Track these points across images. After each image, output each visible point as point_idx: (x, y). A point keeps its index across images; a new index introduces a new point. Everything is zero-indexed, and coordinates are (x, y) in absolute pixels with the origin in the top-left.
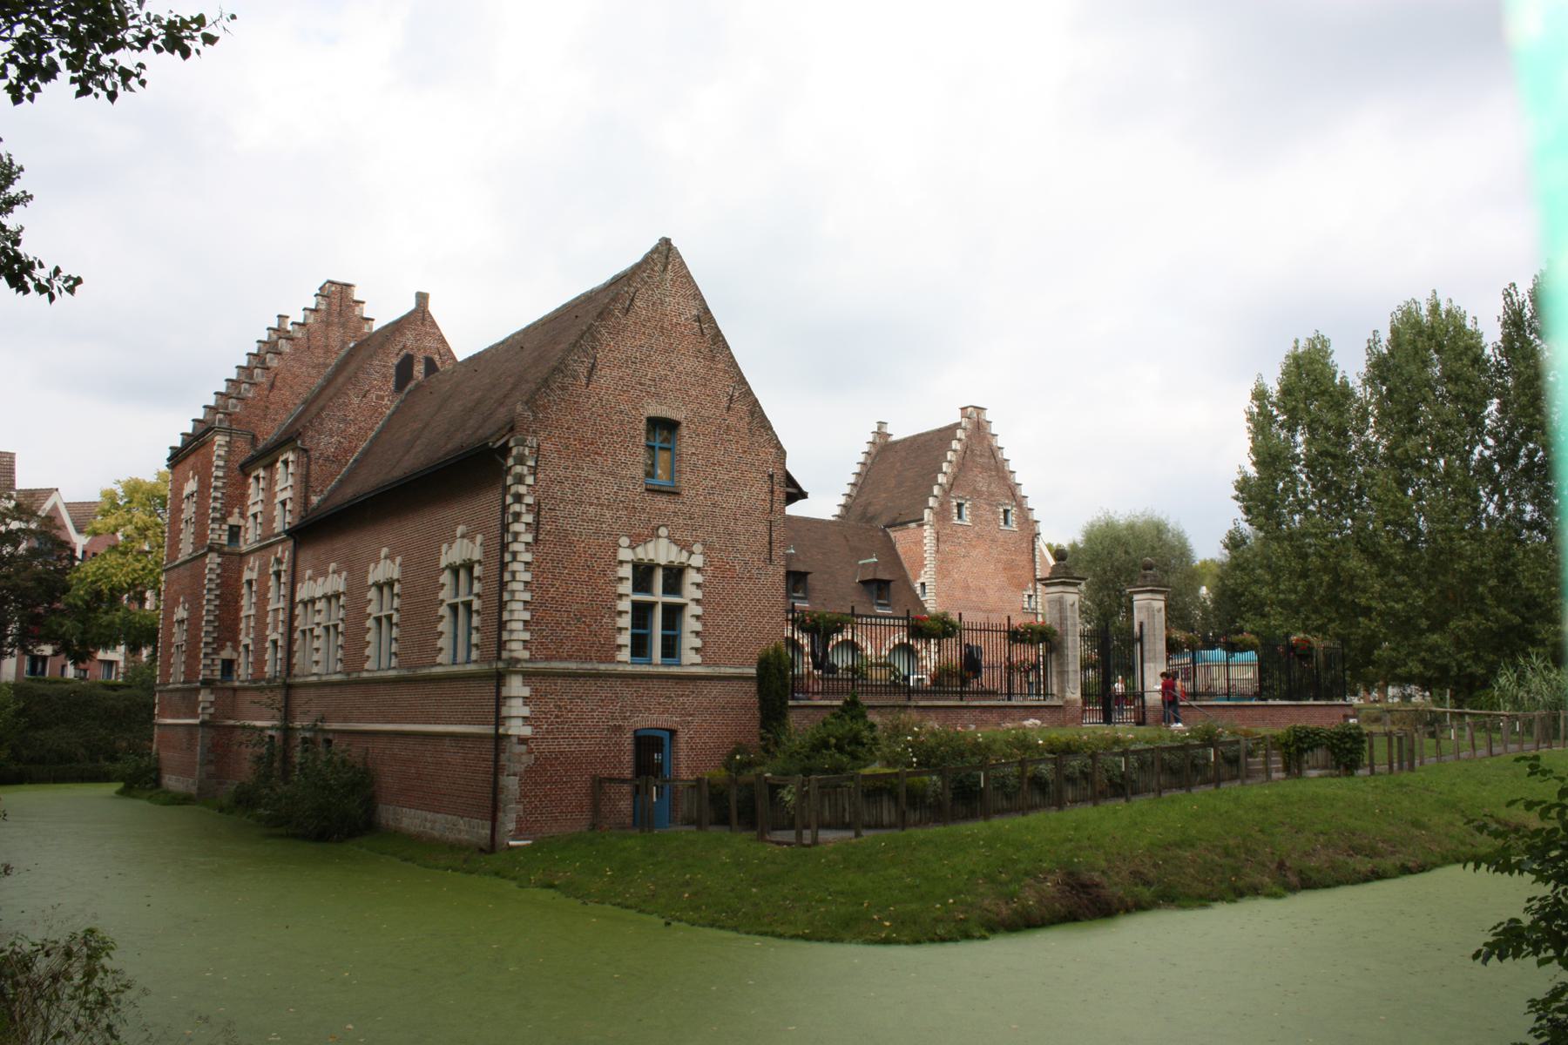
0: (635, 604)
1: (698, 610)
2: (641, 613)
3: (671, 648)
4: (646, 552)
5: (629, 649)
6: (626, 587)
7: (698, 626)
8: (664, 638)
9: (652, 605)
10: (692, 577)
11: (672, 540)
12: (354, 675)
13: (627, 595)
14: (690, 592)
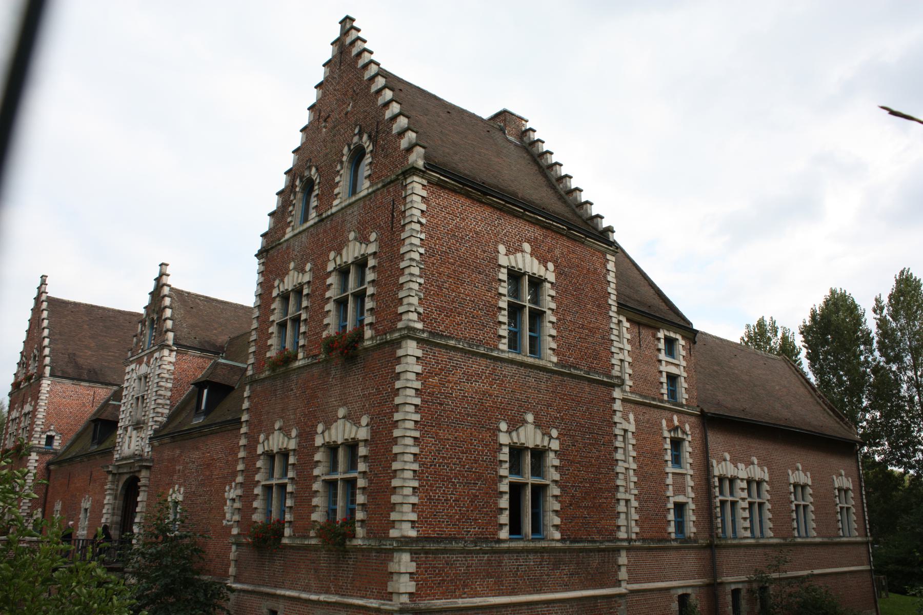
0: (512, 485)
2: (516, 490)
5: (507, 528)
6: (504, 471)
7: (557, 506)
10: (552, 460)
11: (537, 424)
12: (789, 540)
13: (506, 477)
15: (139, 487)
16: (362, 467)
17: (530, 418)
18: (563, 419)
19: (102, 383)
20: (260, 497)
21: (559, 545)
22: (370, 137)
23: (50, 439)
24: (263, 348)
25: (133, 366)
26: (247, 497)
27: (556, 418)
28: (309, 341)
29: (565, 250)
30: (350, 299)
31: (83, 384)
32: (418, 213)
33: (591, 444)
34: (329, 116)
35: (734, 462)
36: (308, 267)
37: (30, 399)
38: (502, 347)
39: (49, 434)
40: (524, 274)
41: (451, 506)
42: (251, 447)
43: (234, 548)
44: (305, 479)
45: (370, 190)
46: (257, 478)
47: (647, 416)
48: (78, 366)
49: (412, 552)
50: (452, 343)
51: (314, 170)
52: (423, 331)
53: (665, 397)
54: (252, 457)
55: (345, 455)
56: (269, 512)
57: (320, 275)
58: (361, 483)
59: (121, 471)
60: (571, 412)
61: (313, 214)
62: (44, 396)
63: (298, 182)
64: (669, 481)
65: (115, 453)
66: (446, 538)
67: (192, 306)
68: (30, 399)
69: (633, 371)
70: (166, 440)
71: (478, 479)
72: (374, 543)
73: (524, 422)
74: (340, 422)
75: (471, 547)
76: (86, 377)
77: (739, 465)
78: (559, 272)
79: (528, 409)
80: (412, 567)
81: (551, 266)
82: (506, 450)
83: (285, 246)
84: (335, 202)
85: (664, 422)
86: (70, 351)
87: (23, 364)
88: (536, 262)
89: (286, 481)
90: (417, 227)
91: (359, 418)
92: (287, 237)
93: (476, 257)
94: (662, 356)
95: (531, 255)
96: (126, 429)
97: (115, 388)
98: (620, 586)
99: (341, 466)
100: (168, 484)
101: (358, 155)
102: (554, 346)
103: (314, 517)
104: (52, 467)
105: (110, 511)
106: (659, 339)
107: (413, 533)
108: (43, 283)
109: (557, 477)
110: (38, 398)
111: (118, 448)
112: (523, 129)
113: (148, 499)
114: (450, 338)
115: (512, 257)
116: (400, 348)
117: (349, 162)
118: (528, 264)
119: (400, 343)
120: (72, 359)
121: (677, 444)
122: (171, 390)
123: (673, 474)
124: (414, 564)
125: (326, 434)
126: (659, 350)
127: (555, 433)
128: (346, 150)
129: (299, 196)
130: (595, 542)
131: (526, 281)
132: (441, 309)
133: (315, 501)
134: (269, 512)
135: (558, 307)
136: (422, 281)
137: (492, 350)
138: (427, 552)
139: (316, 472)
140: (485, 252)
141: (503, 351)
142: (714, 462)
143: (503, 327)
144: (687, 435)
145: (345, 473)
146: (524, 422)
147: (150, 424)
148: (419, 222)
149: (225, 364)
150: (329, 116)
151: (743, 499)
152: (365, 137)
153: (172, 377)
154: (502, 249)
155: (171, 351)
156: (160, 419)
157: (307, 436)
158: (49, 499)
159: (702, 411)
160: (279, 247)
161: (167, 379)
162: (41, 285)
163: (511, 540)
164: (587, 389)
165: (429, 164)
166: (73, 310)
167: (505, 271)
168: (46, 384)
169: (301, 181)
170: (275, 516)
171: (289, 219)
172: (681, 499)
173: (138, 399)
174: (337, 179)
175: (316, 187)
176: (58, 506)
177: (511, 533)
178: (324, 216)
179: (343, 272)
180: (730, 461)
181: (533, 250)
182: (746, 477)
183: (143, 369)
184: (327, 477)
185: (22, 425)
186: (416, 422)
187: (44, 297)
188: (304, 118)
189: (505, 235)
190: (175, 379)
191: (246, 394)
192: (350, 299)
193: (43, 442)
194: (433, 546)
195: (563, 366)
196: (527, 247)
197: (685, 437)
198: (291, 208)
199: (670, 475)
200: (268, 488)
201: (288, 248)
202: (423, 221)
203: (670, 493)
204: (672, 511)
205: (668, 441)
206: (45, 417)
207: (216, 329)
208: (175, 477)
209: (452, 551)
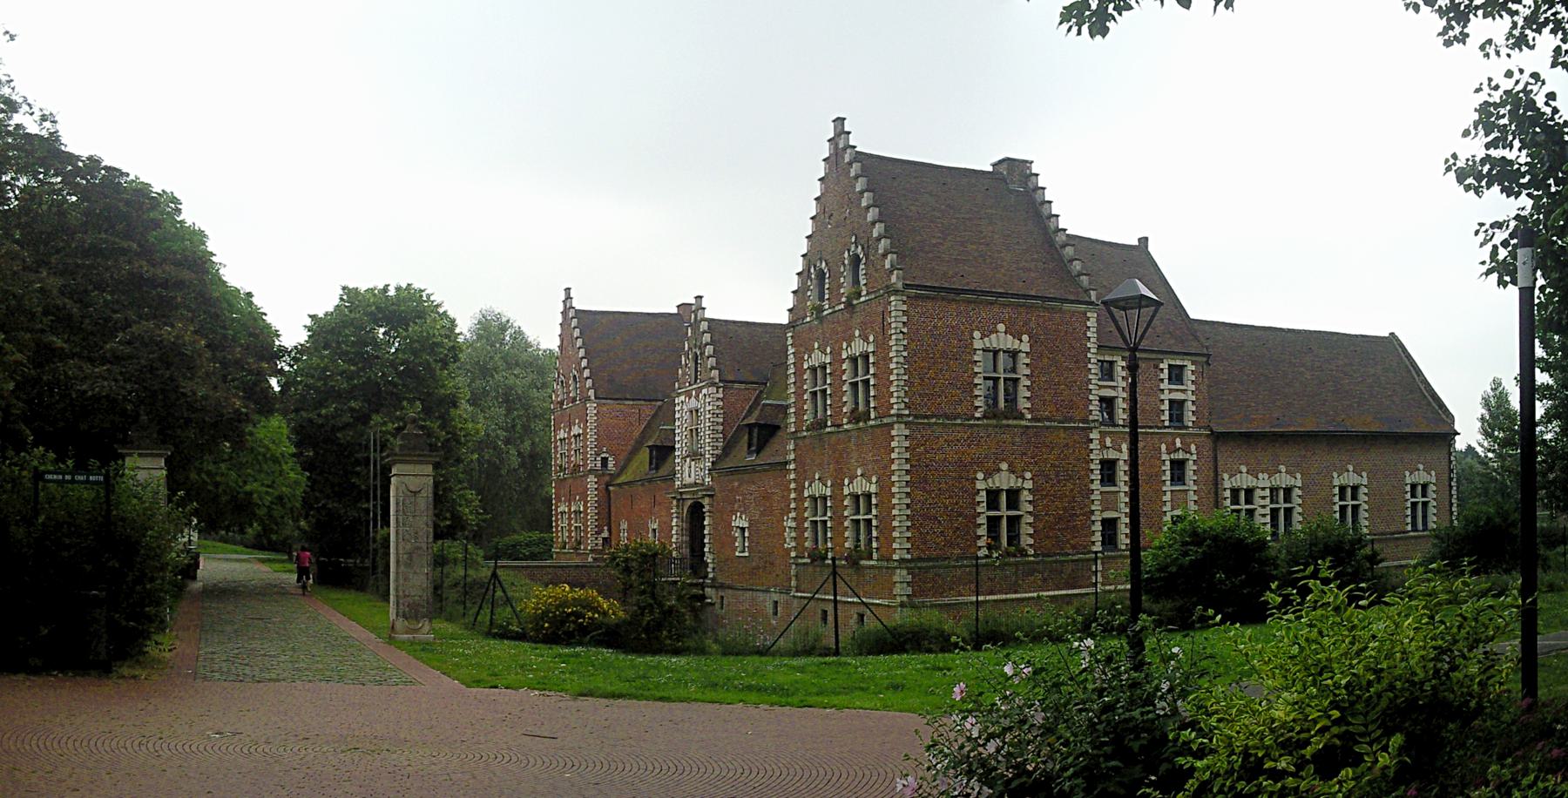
1: (1031, 520)
2: (993, 523)
4: (994, 483)
11: (1012, 470)
16: (874, 512)
17: (1004, 466)
21: (1032, 559)
22: (863, 248)
23: (605, 461)
24: (800, 413)
25: (682, 398)
26: (799, 529)
32: (901, 325)
35: (1253, 472)
36: (828, 350)
40: (1000, 350)
42: (799, 490)
43: (794, 567)
44: (839, 519)
49: (907, 568)
52: (909, 416)
53: (1167, 423)
54: (800, 499)
57: (837, 359)
58: (874, 523)
59: (684, 496)
62: (592, 418)
63: (812, 270)
71: (960, 516)
73: (999, 470)
74: (859, 478)
78: (1034, 341)
81: (1025, 338)
82: (984, 493)
85: (1163, 447)
90: (901, 336)
94: (1165, 385)
95: (1006, 333)
96: (684, 459)
97: (659, 403)
99: (862, 511)
101: (856, 260)
104: (611, 488)
107: (909, 557)
108: (568, 297)
115: (986, 339)
121: (1178, 466)
123: (1172, 491)
127: (1028, 475)
128: (846, 255)
135: (1032, 371)
136: (906, 377)
138: (919, 568)
139: (846, 514)
146: (999, 470)
147: (707, 456)
148: (901, 332)
151: (1264, 507)
152: (860, 247)
154: (977, 334)
156: (716, 452)
157: (838, 485)
159: (1211, 431)
162: (566, 299)
164: (1062, 435)
168: (591, 407)
173: (691, 430)
174: (842, 280)
176: (624, 526)
179: (854, 360)
182: (1269, 485)
183: (693, 403)
184: (855, 517)
185: (573, 446)
186: (907, 482)
189: (980, 322)
190: (724, 413)
194: (924, 565)
197: (1188, 456)
202: (905, 330)
203: (1167, 508)
205: (1168, 463)
208: (736, 506)
209: (940, 567)
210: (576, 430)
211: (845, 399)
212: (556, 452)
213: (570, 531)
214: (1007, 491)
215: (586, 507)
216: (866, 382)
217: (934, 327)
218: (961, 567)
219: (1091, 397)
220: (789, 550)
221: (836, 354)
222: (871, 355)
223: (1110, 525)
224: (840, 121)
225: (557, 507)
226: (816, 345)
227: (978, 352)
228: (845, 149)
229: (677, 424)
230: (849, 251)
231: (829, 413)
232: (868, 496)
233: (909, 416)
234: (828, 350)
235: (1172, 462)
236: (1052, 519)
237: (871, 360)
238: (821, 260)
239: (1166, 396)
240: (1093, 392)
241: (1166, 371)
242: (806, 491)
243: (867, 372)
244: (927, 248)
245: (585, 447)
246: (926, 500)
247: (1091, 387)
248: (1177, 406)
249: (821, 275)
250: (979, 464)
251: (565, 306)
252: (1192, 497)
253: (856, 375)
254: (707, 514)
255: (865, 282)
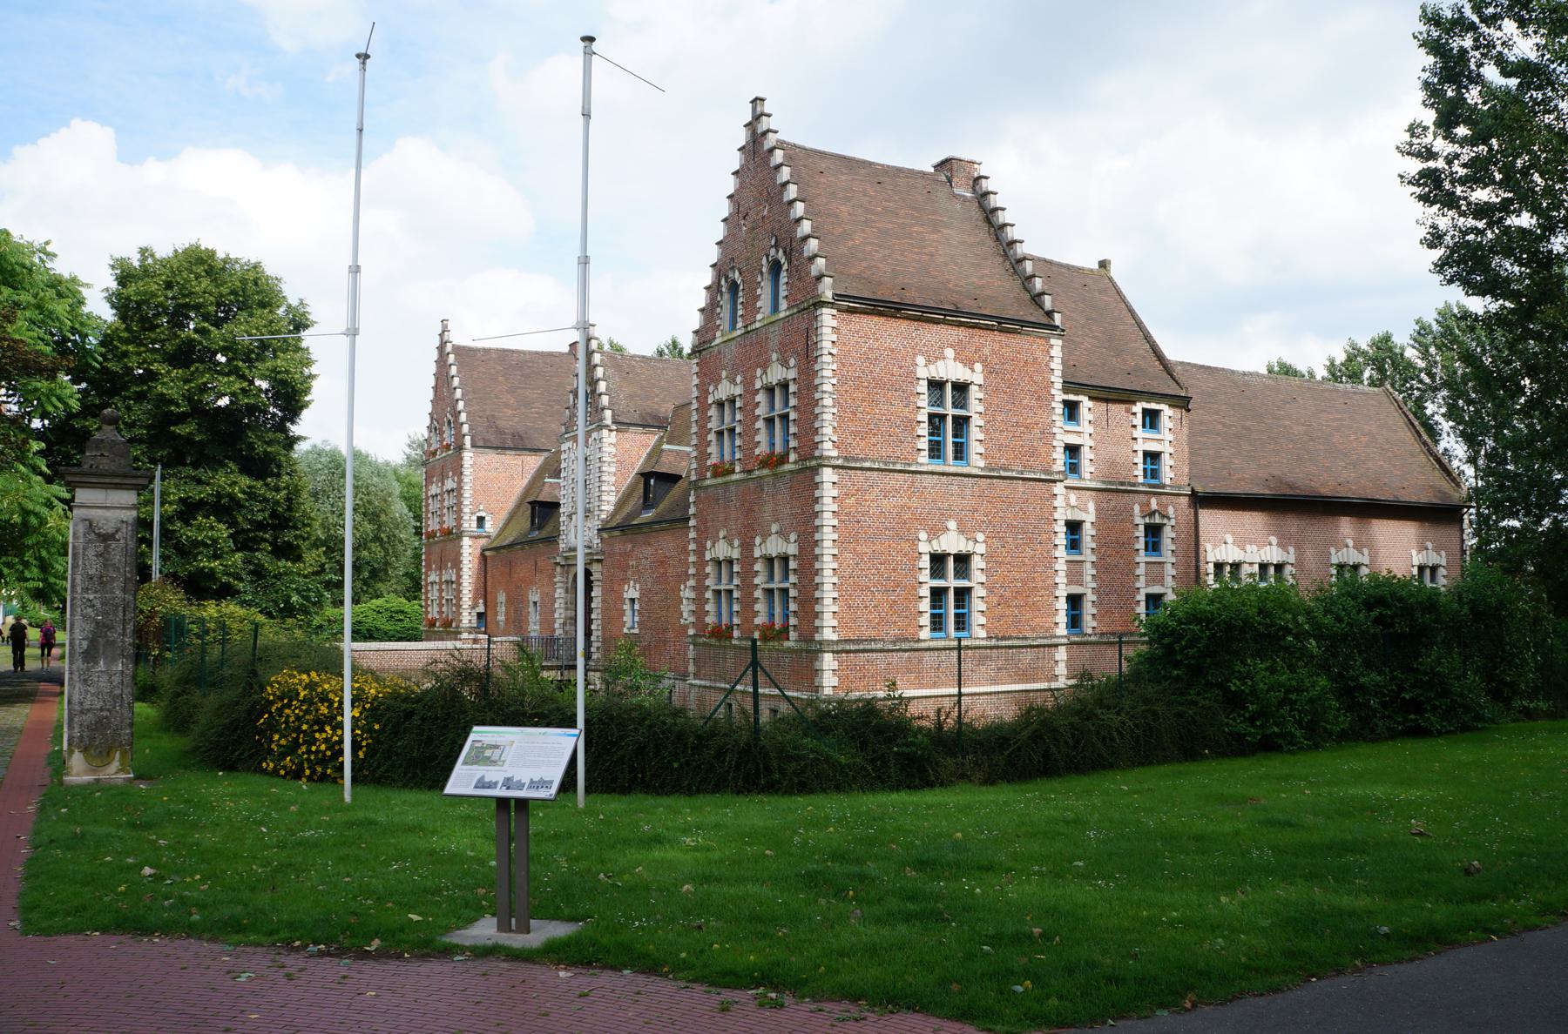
3: (962, 622)
6: (925, 576)
7: (983, 607)
8: (957, 615)
9: (945, 590)
10: (977, 563)
11: (961, 531)
14: (977, 577)
15: (592, 582)
16: (793, 579)
17: (952, 525)
18: (990, 522)
19: (530, 450)
20: (712, 601)
21: (984, 643)
22: (785, 252)
23: (481, 520)
26: (700, 601)
27: (983, 522)
28: (745, 455)
29: (997, 346)
30: (777, 420)
31: (508, 452)
33: (1024, 544)
34: (747, 214)
35: (1241, 543)
36: (739, 379)
37: (451, 474)
38: (920, 460)
39: (479, 514)
40: (947, 381)
41: (870, 612)
42: (700, 551)
43: (691, 647)
44: (748, 587)
45: (788, 313)
46: (707, 582)
47: (1113, 503)
48: (500, 432)
50: (867, 465)
51: (737, 273)
52: (838, 458)
53: (1141, 479)
54: (701, 564)
55: (780, 567)
56: (719, 614)
57: (750, 392)
58: (793, 593)
60: (1001, 514)
61: (740, 325)
62: (467, 471)
63: (723, 282)
64: (1141, 570)
65: (560, 542)
66: (866, 640)
67: (627, 370)
68: (451, 474)
69: (1096, 454)
70: (616, 533)
71: (897, 587)
72: (804, 646)
75: (891, 647)
76: (509, 443)
77: (1248, 547)
78: (989, 371)
79: (950, 516)
80: (835, 665)
81: (978, 367)
83: (716, 349)
84: (759, 317)
85: (1137, 508)
86: (488, 413)
87: (435, 429)
88: (960, 365)
89: (732, 587)
91: (788, 534)
92: (717, 341)
93: (893, 375)
94: (1139, 433)
97: (546, 454)
98: (1057, 680)
100: (622, 580)
101: (776, 267)
102: (982, 450)
103: (758, 621)
105: (562, 606)
106: (1134, 414)
109: (983, 579)
110: (461, 473)
111: (564, 537)
112: (976, 175)
113: (603, 594)
114: (863, 460)
115: (932, 367)
116: (817, 474)
117: (769, 273)
118: (951, 369)
119: (817, 470)
120: (491, 420)
121: (1154, 531)
122: (615, 474)
123: (1146, 563)
124: (836, 662)
125: (763, 546)
126: (1134, 426)
128: (764, 261)
129: (726, 296)
130: (1026, 638)
131: (949, 387)
132: (855, 434)
133: (758, 607)
134: (719, 614)
135: (986, 409)
136: (835, 411)
137: (909, 465)
139: (757, 581)
140: (901, 367)
141: (921, 464)
142: (1209, 547)
143: (922, 439)
144: (1169, 519)
145: (780, 582)
148: (830, 354)
149: (670, 451)
150: (747, 214)
152: (781, 251)
153: (614, 460)
154: (920, 360)
155: (611, 431)
157: (747, 547)
158: (489, 589)
160: (711, 350)
161: (609, 463)
162: (443, 332)
163: (932, 639)
164: (1021, 489)
165: (837, 295)
166: (483, 358)
167: (926, 382)
168: (468, 456)
169: (726, 281)
170: (725, 620)
171: (718, 322)
172: (1156, 590)
174: (759, 291)
175: (741, 294)
176: (502, 598)
177: (934, 630)
178: (749, 329)
179: (770, 390)
180: (1234, 543)
181: (957, 354)
184: (766, 586)
185: (446, 504)
187: (449, 348)
188: (725, 209)
191: (692, 499)
192: (777, 420)
193: (474, 524)
195: (990, 470)
196: (950, 353)
197: (1165, 521)
198: (718, 310)
199: (1142, 566)
200: (718, 593)
201: (719, 353)
202: (834, 351)
203: (1141, 583)
204: (1143, 604)
205: (1142, 528)
206: (472, 495)
207: (657, 396)
209: (872, 651)
210: (450, 484)
211: (757, 438)
212: (428, 511)
213: (441, 605)
214: (955, 555)
215: (459, 577)
216: (785, 417)
217: (870, 349)
218: (897, 651)
219: (1055, 443)
220: (686, 627)
221: (748, 383)
222: (791, 383)
223: (1074, 601)
224: (757, 101)
225: (427, 576)
226: (724, 374)
227: (921, 382)
228: (765, 133)
229: (562, 475)
230: (767, 256)
231: (737, 456)
232: (785, 559)
233: (838, 458)
234: (739, 379)
235: (1147, 527)
236: (1008, 594)
237: (792, 388)
238: (733, 268)
239: (1141, 446)
240: (1058, 437)
241: (1140, 416)
242: (707, 553)
243: (786, 404)
244: (860, 255)
245: (459, 503)
246: (857, 564)
247: (1055, 430)
248: (1152, 457)
249: (734, 287)
250: (921, 521)
251: (442, 340)
252: (1170, 570)
253: (772, 407)
254: (595, 583)
255: (785, 293)
